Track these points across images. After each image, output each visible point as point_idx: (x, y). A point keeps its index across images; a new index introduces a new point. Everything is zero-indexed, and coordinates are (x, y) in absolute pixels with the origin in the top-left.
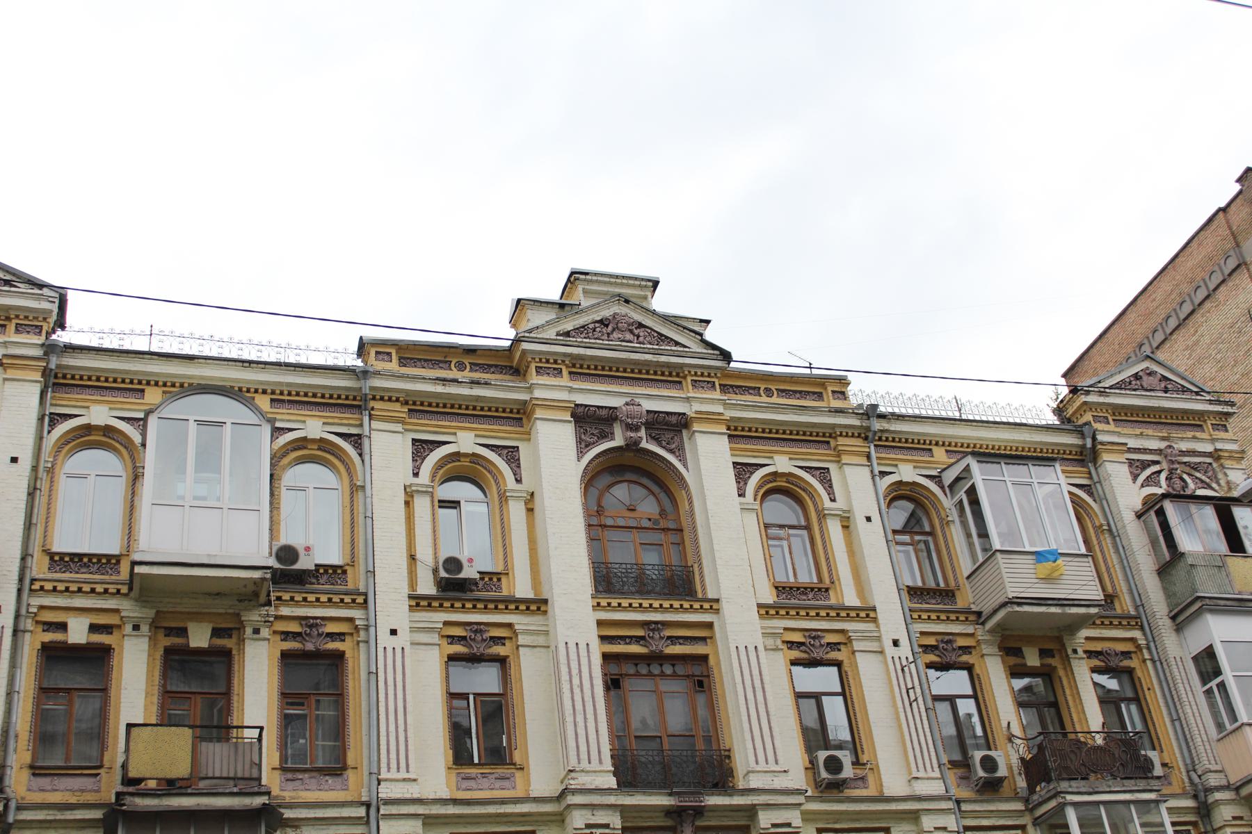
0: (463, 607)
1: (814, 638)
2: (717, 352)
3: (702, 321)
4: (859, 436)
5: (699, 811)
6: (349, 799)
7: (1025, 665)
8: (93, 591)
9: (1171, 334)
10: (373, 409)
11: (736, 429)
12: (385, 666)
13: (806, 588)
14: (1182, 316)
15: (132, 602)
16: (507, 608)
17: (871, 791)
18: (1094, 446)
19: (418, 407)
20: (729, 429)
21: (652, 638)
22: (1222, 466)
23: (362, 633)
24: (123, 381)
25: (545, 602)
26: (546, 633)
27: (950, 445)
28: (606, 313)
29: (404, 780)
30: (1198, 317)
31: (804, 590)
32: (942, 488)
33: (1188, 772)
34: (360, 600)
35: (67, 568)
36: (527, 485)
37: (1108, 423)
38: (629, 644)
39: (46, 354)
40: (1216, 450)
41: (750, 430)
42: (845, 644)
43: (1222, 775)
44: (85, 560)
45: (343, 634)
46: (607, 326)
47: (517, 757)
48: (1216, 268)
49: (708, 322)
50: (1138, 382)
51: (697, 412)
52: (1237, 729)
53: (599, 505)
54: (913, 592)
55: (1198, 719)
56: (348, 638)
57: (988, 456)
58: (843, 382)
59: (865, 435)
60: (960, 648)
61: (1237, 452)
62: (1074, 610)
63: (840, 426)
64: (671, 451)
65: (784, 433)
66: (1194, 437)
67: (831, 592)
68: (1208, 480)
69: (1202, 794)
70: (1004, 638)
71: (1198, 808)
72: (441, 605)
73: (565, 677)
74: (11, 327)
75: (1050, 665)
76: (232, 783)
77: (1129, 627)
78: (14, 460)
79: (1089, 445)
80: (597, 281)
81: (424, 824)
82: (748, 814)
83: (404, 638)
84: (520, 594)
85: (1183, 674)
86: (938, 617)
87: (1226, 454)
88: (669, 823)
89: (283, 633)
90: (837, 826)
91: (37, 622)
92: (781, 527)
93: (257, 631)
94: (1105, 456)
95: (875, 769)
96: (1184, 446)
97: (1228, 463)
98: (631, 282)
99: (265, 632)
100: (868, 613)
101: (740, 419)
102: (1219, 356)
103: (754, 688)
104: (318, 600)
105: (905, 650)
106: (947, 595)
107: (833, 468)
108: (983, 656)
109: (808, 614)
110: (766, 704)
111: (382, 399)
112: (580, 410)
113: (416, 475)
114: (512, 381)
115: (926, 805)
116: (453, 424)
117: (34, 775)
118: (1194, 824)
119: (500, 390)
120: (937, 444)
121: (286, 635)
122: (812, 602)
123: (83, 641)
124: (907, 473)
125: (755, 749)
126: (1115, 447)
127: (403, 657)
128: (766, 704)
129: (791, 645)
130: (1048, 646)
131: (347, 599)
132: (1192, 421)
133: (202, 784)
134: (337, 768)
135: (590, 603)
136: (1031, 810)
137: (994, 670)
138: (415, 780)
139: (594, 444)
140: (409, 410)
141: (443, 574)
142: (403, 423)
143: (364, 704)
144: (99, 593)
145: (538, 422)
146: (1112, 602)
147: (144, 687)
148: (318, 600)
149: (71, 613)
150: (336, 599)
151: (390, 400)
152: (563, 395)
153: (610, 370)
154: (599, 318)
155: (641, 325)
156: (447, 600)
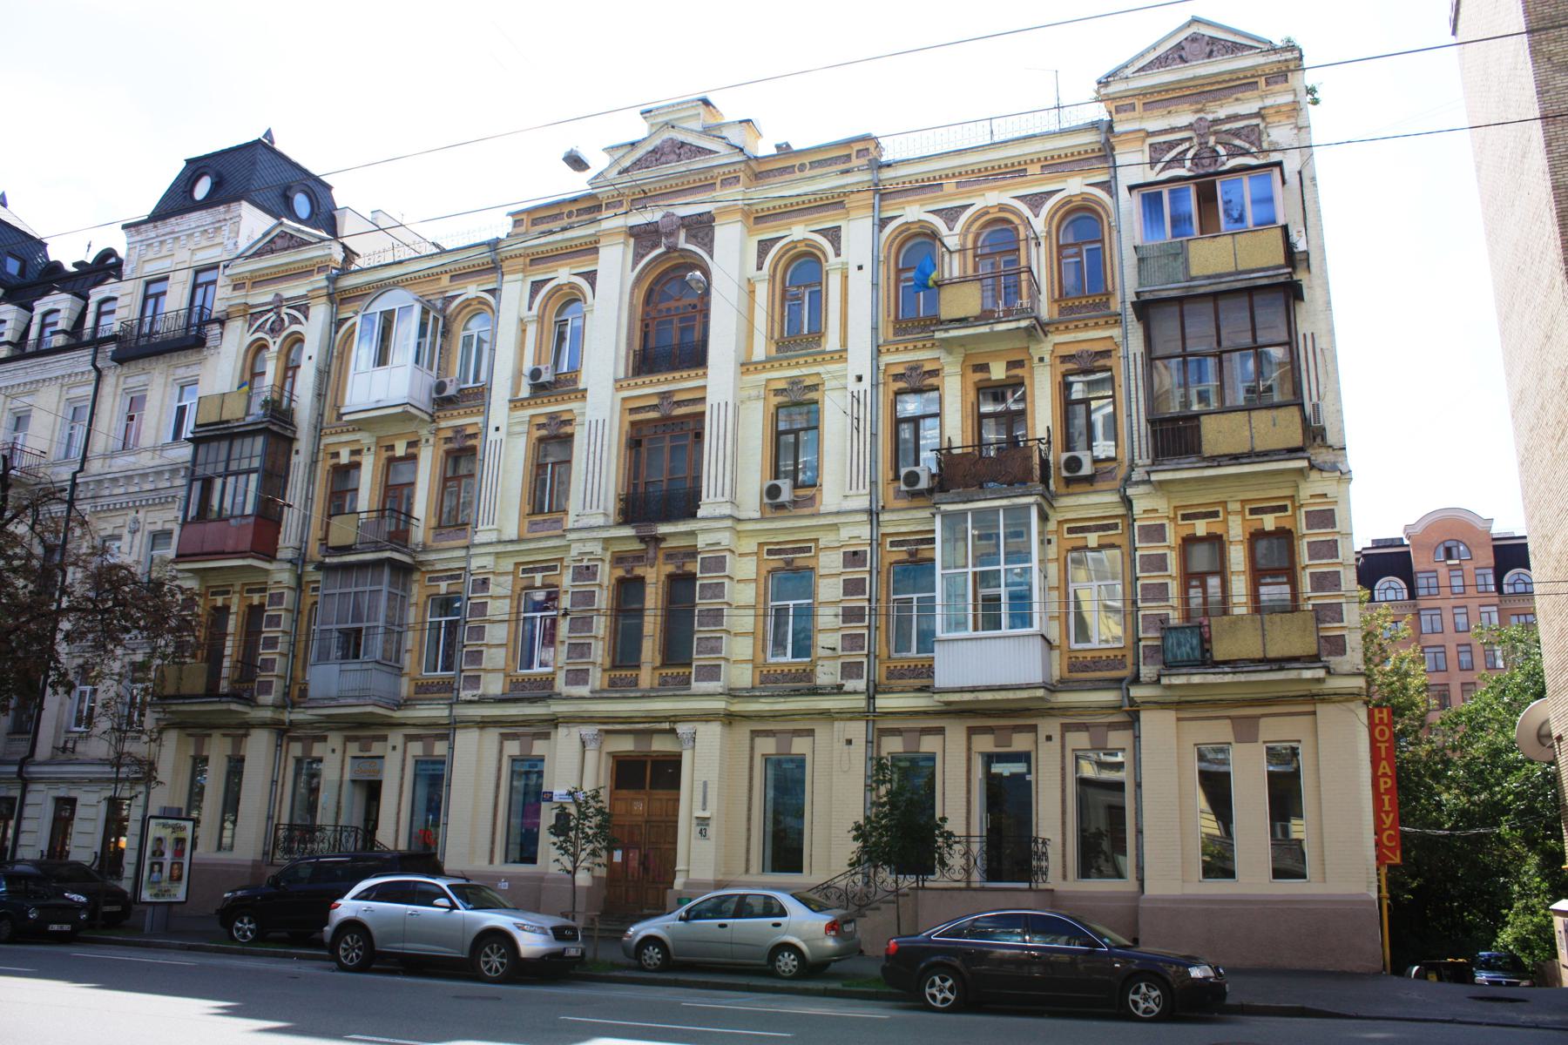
3: (741, 122)
5: (658, 539)
7: (989, 379)
18: (1108, 140)
61: (1286, 104)
66: (1237, 100)
68: (1247, 146)
75: (1017, 376)
79: (1102, 138)
83: (503, 430)
88: (643, 546)
96: (1222, 114)
100: (841, 354)
105: (866, 383)
113: (530, 308)
124: (914, 212)
131: (475, 410)
142: (523, 271)
152: (619, 222)
154: (650, 149)
155: (683, 144)
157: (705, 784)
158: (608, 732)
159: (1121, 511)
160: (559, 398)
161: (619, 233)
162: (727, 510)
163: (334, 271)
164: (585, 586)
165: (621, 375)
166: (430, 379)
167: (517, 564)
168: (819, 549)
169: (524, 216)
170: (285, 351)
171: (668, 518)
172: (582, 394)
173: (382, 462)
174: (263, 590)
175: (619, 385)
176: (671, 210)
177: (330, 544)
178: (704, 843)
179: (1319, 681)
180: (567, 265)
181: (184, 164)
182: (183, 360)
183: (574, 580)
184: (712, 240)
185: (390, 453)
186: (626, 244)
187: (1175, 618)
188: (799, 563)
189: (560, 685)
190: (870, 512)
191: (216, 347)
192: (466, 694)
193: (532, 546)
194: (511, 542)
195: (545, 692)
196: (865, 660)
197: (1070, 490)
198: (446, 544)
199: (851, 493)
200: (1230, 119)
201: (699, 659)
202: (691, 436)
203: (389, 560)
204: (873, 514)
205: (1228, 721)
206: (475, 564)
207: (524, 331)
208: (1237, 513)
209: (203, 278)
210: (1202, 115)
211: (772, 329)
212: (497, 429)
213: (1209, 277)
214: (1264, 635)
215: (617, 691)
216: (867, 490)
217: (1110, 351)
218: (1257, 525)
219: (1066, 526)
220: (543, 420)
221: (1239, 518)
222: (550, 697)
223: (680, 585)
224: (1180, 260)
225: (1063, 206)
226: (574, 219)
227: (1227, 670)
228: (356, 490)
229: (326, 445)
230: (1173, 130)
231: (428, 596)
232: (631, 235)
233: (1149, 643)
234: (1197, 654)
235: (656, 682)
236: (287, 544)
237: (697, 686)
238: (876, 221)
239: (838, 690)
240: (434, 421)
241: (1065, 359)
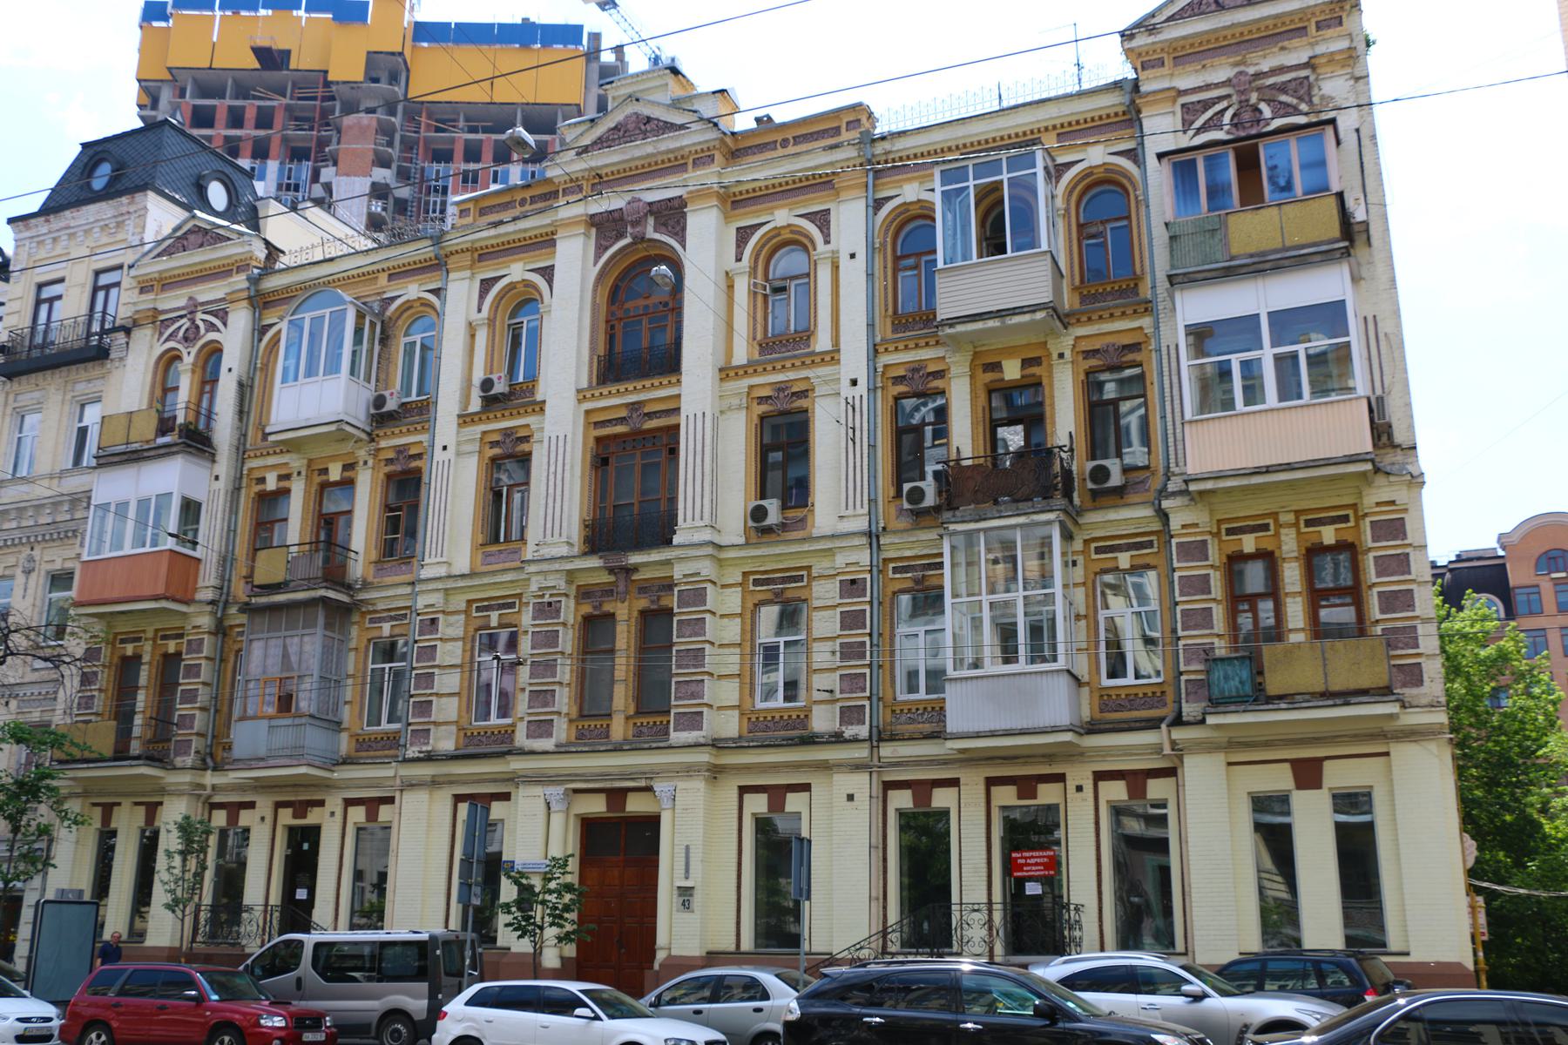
3: (714, 93)
5: (630, 570)
7: (1003, 380)
18: (1133, 102)
61: (1341, 51)
66: (1283, 48)
68: (1295, 101)
70: (976, 353)
75: (1034, 375)
79: (1126, 99)
88: (612, 578)
90: (762, 569)
96: (1265, 67)
100: (832, 357)
112: (597, 219)
113: (480, 310)
124: (910, 192)
126: (1160, 96)
131: (419, 427)
139: (611, 246)
142: (471, 267)
152: (578, 210)
154: (613, 125)
155: (649, 120)
157: (687, 848)
158: (576, 791)
159: (1156, 526)
160: (515, 412)
161: (577, 223)
162: (706, 535)
163: (256, 271)
164: (546, 625)
165: (585, 384)
166: (367, 394)
167: (469, 602)
168: (811, 578)
169: (471, 205)
170: (200, 363)
171: (640, 546)
172: (540, 407)
173: (314, 488)
174: (181, 636)
175: (582, 395)
176: (637, 195)
177: (256, 583)
178: (686, 916)
179: (1391, 717)
180: (520, 260)
181: (79, 148)
182: (83, 375)
183: (534, 618)
184: (684, 229)
186: (587, 235)
187: (1221, 648)
188: (789, 595)
189: (521, 739)
190: (869, 534)
192: (412, 752)
193: (486, 580)
194: (463, 576)
195: (504, 748)
196: (867, 703)
197: (1097, 504)
198: (389, 580)
199: (850, 512)
200: (1275, 71)
201: (678, 706)
202: (665, 453)
203: (324, 600)
204: (872, 537)
206: (421, 602)
207: (473, 336)
208: (1290, 526)
209: (105, 280)
210: (1242, 68)
211: (755, 329)
212: (445, 448)
213: (1252, 256)
214: (1325, 665)
215: (585, 745)
216: (866, 510)
217: (1140, 344)
218: (1314, 539)
219: (1093, 545)
220: (496, 437)
221: (1293, 531)
222: (509, 753)
224: (1218, 236)
225: (1083, 179)
226: (527, 207)
227: (1283, 706)
228: (286, 520)
229: (251, 470)
230: (1208, 87)
231: (369, 640)
232: (593, 225)
233: (1193, 677)
234: (1248, 689)
235: (630, 733)
236: (207, 584)
237: (677, 737)
238: (871, 202)
239: (837, 739)
240: (373, 440)
241: (1088, 354)
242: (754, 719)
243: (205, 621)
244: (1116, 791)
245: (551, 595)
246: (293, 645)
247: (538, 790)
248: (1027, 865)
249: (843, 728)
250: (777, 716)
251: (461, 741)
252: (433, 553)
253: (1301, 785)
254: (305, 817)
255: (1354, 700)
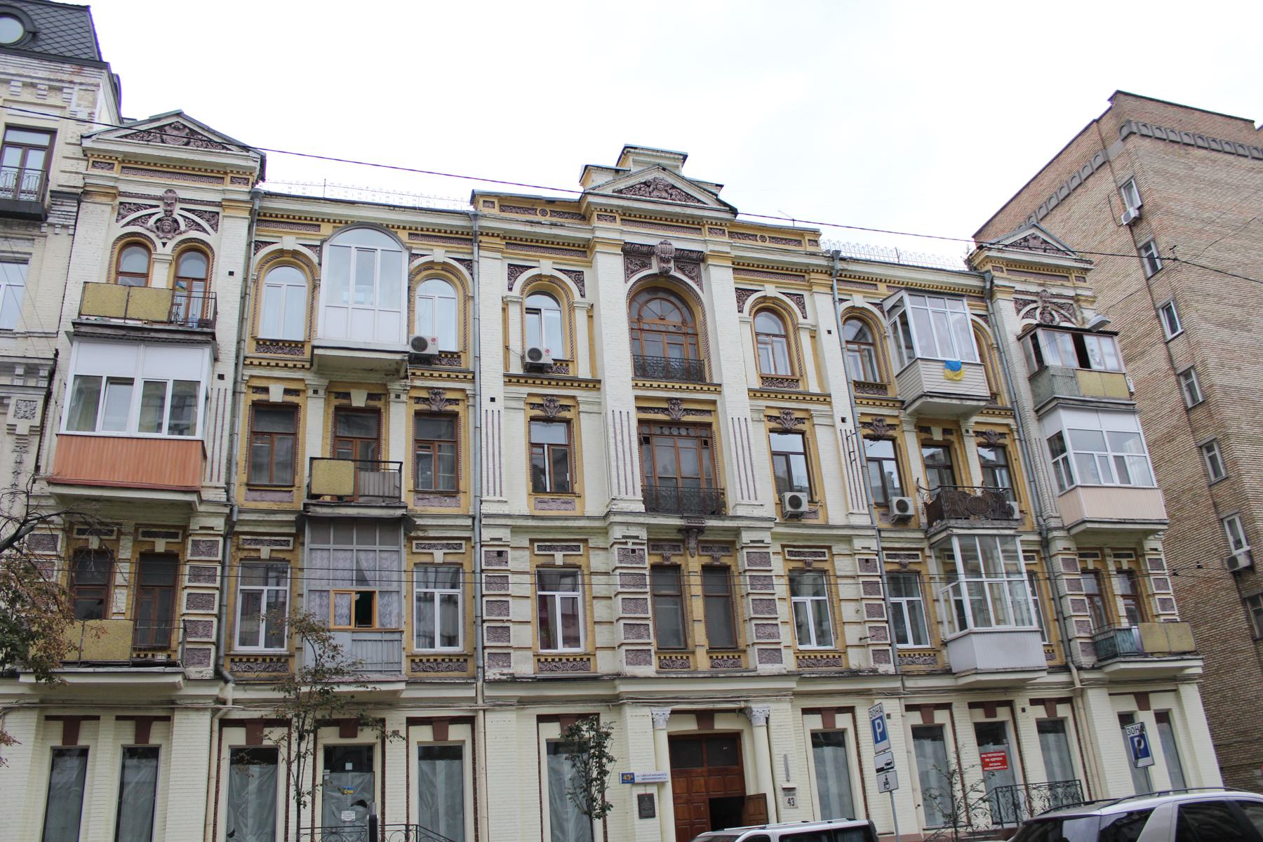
0: (542, 383)
1: (787, 414)
2: (728, 208)
3: (717, 185)
4: (826, 273)
5: (701, 530)
6: (461, 513)
7: (932, 439)
8: (286, 366)
9: (1052, 210)
10: (480, 242)
11: (738, 264)
12: (487, 422)
13: (782, 379)
14: (1061, 198)
15: (313, 374)
16: (572, 385)
17: (820, 521)
18: (991, 287)
19: (513, 241)
20: (733, 264)
21: (673, 409)
22: (1080, 307)
23: (471, 400)
24: (306, 219)
25: (599, 381)
26: (599, 404)
27: (890, 282)
28: (649, 177)
29: (499, 501)
30: (1072, 198)
31: (781, 380)
32: (883, 312)
33: (1037, 517)
34: (470, 376)
35: (268, 350)
36: (589, 298)
37: (1003, 272)
38: (657, 413)
39: (252, 198)
40: (1077, 295)
41: (748, 265)
42: (808, 419)
43: (1059, 520)
44: (281, 344)
45: (458, 400)
46: (649, 186)
47: (577, 488)
48: (1088, 164)
49: (722, 186)
50: (1026, 244)
51: (711, 251)
52: (1073, 489)
53: (639, 315)
54: (858, 385)
55: (1047, 481)
56: (461, 403)
57: (917, 291)
58: (816, 233)
59: (830, 272)
60: (888, 425)
61: (1091, 297)
62: (969, 403)
63: (813, 265)
64: (692, 278)
65: (773, 268)
66: (1062, 285)
67: (800, 383)
69: (1045, 532)
70: (918, 418)
71: (1041, 541)
72: (526, 382)
73: (611, 434)
74: (228, 179)
75: (949, 440)
76: (381, 499)
77: (1006, 416)
78: (231, 273)
79: (988, 286)
80: (643, 154)
81: (511, 532)
82: (734, 533)
83: (500, 404)
84: (581, 376)
85: (1040, 450)
86: (874, 403)
87: (1083, 298)
88: (680, 537)
89: (416, 398)
91: (249, 387)
92: (768, 335)
93: (398, 396)
94: (999, 295)
95: (824, 506)
96: (1054, 291)
97: (1083, 305)
98: (668, 155)
99: (404, 397)
100: (825, 398)
101: (741, 257)
102: (1084, 228)
103: (743, 447)
104: (440, 376)
105: (850, 425)
106: (881, 388)
107: (806, 294)
108: (903, 431)
109: (783, 397)
110: (751, 458)
111: (487, 235)
112: (628, 246)
113: (510, 289)
114: (580, 224)
115: (857, 532)
116: (537, 254)
117: (249, 490)
118: (1037, 552)
119: (572, 231)
120: (881, 281)
121: (418, 400)
122: (786, 389)
123: (280, 401)
124: (859, 300)
125: (741, 489)
127: (499, 417)
128: (751, 458)
129: (770, 418)
130: (948, 427)
131: (461, 376)
132: (1060, 273)
133: (361, 500)
134: (452, 492)
135: (631, 383)
136: (929, 538)
137: (910, 441)
138: (506, 502)
140: (507, 243)
141: (528, 360)
142: (502, 252)
143: (472, 449)
144: (290, 368)
145: (598, 254)
146: (995, 398)
147: (321, 432)
148: (440, 376)
149: (272, 381)
150: (453, 375)
151: (493, 235)
153: (651, 218)
155: (673, 187)
156: (530, 378)
157: (785, 757)
185: (345, 402)
188: (816, 565)
191: (64, 226)
192: (492, 674)
205: (1132, 696)
206: (487, 534)
213: (1092, 397)
217: (1005, 434)
223: (716, 573)
236: (215, 483)
242: (801, 658)
243: (219, 524)
244: (1040, 712)
245: (633, 544)
246: (366, 561)
247: (646, 711)
248: (992, 762)
249: (877, 666)
250: (818, 655)
251: (537, 667)
252: (491, 491)
253: (1141, 709)
254: (355, 736)
255: (1185, 657)
